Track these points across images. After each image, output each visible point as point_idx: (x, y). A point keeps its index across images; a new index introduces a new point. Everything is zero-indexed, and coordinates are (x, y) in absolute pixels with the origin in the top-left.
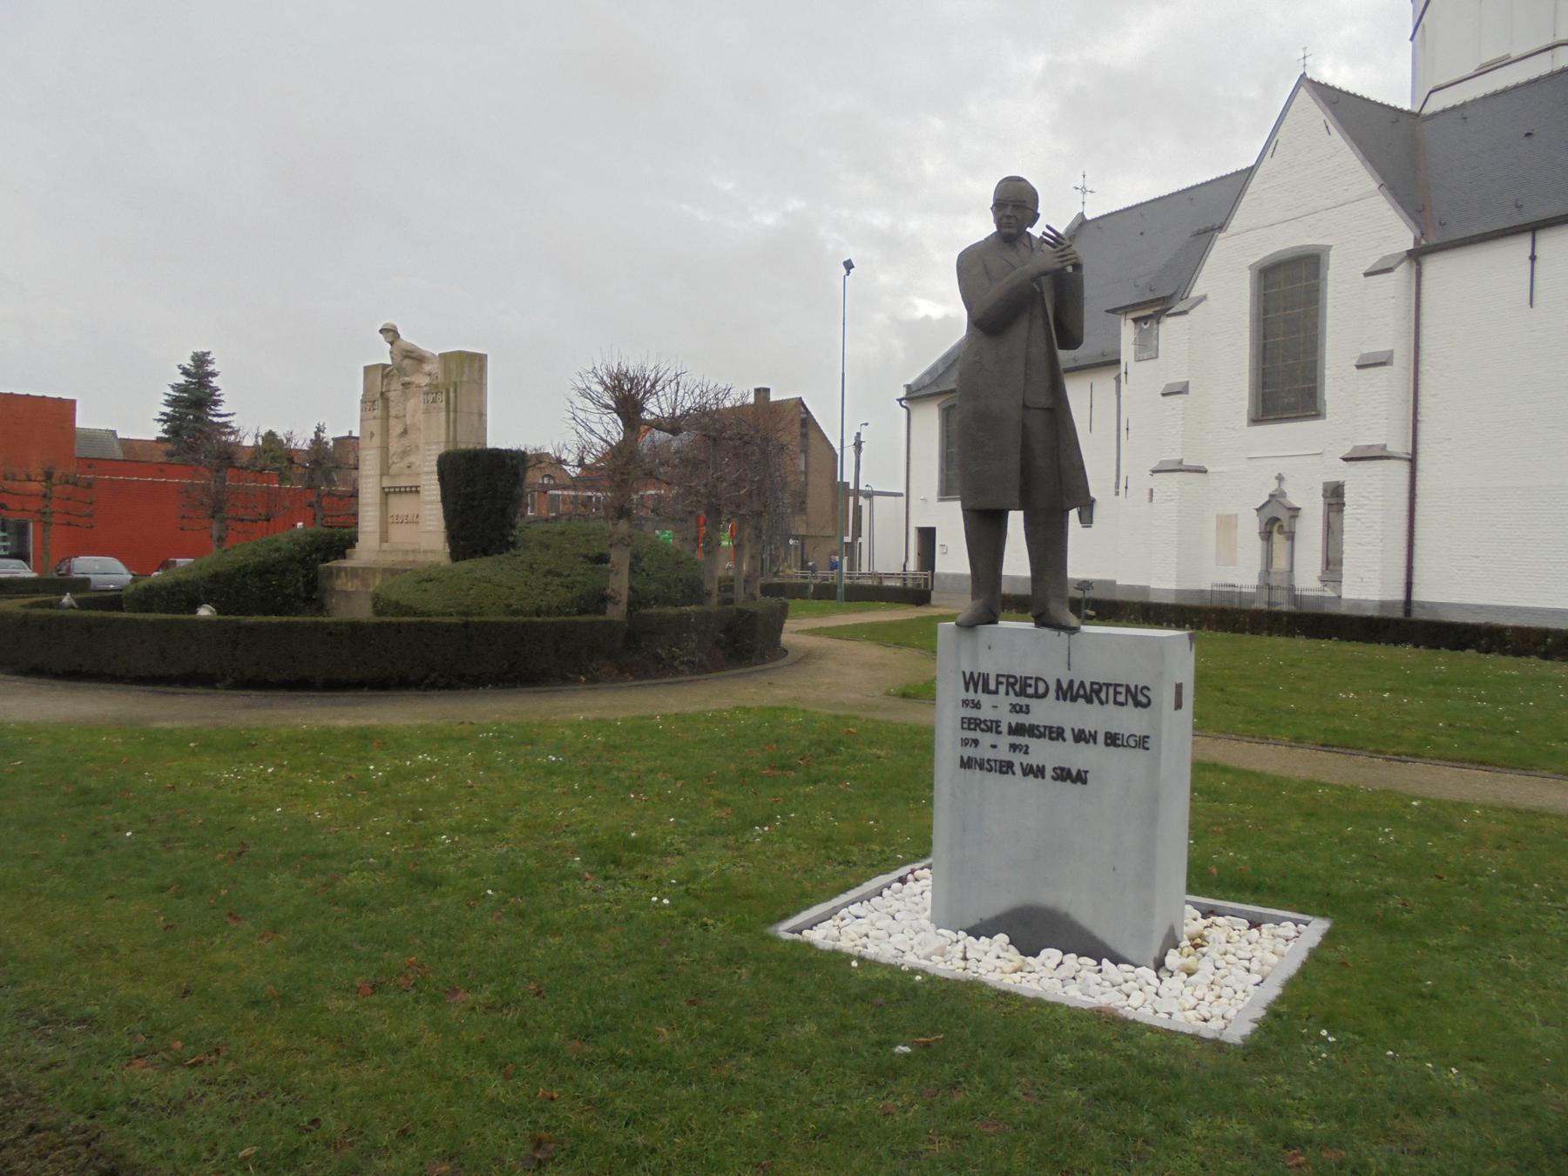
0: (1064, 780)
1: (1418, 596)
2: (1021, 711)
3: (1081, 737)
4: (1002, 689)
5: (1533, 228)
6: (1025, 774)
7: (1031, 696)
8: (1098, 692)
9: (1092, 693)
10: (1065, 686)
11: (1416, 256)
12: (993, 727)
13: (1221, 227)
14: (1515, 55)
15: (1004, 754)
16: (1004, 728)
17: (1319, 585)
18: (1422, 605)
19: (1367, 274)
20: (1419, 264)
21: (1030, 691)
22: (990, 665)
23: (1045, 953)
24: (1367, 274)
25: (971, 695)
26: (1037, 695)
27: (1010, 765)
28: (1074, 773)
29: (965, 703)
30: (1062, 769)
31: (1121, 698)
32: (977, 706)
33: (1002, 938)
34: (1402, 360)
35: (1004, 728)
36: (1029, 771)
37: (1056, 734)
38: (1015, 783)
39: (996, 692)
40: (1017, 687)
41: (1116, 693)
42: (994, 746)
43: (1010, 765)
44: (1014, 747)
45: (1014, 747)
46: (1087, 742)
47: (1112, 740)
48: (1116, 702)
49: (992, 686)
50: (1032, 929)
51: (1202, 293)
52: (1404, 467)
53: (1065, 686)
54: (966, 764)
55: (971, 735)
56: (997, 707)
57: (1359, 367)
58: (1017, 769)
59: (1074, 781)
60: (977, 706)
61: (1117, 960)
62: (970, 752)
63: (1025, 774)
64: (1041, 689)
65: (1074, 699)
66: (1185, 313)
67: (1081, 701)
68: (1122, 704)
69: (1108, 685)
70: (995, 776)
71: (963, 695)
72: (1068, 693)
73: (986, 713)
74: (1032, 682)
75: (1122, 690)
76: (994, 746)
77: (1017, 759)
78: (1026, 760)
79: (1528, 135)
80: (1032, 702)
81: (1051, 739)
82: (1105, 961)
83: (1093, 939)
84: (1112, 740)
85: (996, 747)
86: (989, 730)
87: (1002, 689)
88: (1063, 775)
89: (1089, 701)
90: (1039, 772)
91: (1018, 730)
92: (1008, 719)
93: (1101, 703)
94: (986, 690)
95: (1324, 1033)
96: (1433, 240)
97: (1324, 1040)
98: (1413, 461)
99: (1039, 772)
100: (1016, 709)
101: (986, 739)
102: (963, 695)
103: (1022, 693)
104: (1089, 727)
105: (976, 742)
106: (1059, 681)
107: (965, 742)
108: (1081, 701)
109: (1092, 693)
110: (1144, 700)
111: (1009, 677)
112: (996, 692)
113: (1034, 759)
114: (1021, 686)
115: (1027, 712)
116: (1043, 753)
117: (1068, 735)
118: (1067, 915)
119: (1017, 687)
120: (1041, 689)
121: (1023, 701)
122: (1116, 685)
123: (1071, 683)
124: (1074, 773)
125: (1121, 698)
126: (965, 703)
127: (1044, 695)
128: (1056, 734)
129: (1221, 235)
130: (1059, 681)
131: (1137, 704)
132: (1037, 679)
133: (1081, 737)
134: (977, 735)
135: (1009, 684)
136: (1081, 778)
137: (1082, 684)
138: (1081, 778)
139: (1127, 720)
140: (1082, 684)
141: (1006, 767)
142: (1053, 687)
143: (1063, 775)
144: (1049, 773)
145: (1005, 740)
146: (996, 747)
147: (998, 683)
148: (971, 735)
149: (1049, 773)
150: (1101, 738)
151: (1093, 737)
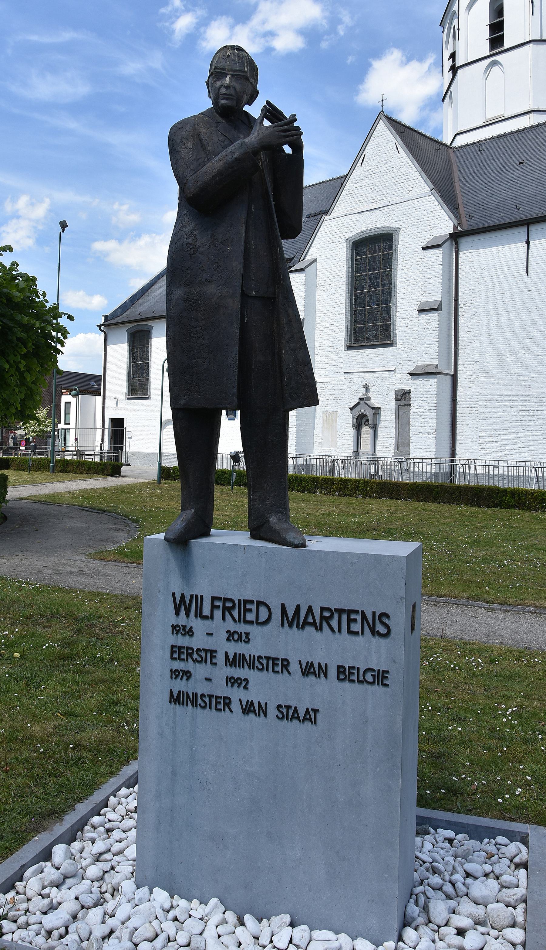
3: (308, 670)
4: (218, 614)
5: (527, 223)
7: (251, 622)
8: (328, 620)
11: (455, 238)
12: (208, 656)
13: (326, 212)
19: (424, 248)
20: (457, 244)
21: (251, 617)
24: (424, 248)
25: (182, 620)
27: (227, 702)
29: (176, 629)
34: (448, 308)
35: (220, 658)
36: (248, 708)
38: (235, 718)
40: (235, 613)
41: (350, 621)
44: (232, 681)
45: (232, 681)
47: (345, 674)
48: (350, 632)
49: (207, 611)
51: (314, 257)
52: (448, 381)
54: (177, 698)
58: (236, 706)
60: (190, 632)
62: (180, 685)
64: (264, 614)
66: (302, 270)
68: (356, 633)
69: (340, 612)
70: (209, 714)
71: (172, 619)
73: (198, 641)
74: (253, 607)
75: (358, 617)
76: (208, 680)
77: (237, 695)
79: (520, 163)
87: (218, 614)
88: (288, 713)
91: (233, 661)
96: (466, 228)
98: (454, 377)
100: (231, 636)
101: (200, 671)
102: (172, 619)
105: (188, 675)
107: (175, 674)
109: (324, 619)
110: (383, 631)
111: (225, 600)
112: (212, 617)
113: (254, 695)
116: (263, 687)
117: (294, 667)
120: (264, 614)
121: (242, 628)
122: (350, 612)
126: (176, 629)
127: (267, 622)
129: (327, 217)
132: (259, 603)
133: (308, 670)
134: (190, 666)
135: (225, 609)
136: (310, 716)
137: (310, 610)
138: (310, 716)
139: (366, 651)
143: (288, 713)
147: (214, 607)
150: (333, 672)
151: (323, 671)
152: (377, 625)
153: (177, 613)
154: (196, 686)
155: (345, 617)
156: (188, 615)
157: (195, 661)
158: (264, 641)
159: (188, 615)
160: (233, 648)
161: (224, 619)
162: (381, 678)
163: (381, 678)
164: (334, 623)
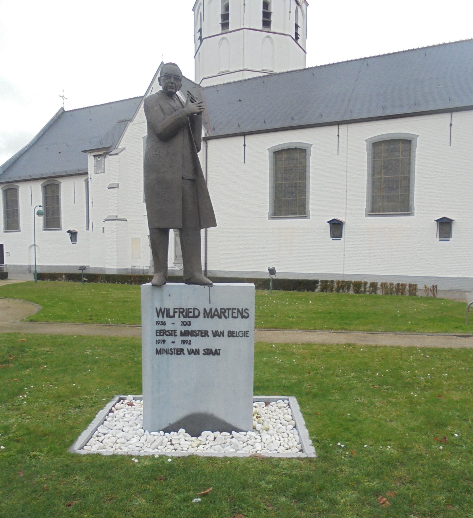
0: (209, 354)
1: (208, 269)
2: (186, 324)
3: (216, 334)
4: (177, 315)
5: (244, 134)
6: (189, 353)
8: (224, 313)
9: (221, 314)
10: (208, 311)
12: (173, 333)
13: (130, 120)
15: (178, 345)
16: (178, 333)
17: (173, 265)
18: (210, 272)
20: (206, 143)
21: (191, 315)
22: (170, 304)
23: (205, 433)
25: (160, 319)
26: (194, 317)
27: (182, 350)
28: (214, 351)
29: (158, 323)
30: (208, 350)
31: (235, 315)
32: (164, 324)
33: (182, 431)
35: (178, 333)
36: (191, 352)
37: (204, 334)
38: (185, 358)
39: (174, 316)
40: (184, 314)
41: (233, 313)
42: (173, 342)
43: (182, 350)
44: (183, 342)
45: (183, 342)
46: (219, 336)
47: (231, 334)
48: (233, 317)
49: (172, 314)
50: (195, 424)
51: (123, 147)
53: (208, 311)
54: (159, 352)
55: (161, 338)
56: (174, 324)
58: (186, 352)
59: (214, 355)
60: (164, 324)
61: (238, 431)
62: (161, 346)
63: (189, 353)
64: (196, 313)
65: (212, 317)
66: (117, 154)
67: (216, 318)
68: (235, 318)
69: (229, 309)
71: (156, 319)
72: (209, 314)
73: (168, 327)
74: (192, 311)
75: (236, 311)
76: (173, 342)
78: (189, 347)
79: (240, 100)
80: (192, 320)
81: (202, 336)
82: (233, 432)
83: (225, 423)
84: (231, 334)
85: (171, 343)
86: (171, 335)
87: (177, 315)
88: (208, 352)
89: (220, 317)
90: (196, 352)
91: (183, 334)
92: (180, 328)
93: (226, 318)
94: (168, 316)
95: (339, 444)
96: (211, 135)
97: (340, 447)
99: (196, 352)
100: (184, 324)
101: (169, 339)
102: (156, 319)
103: (187, 316)
104: (220, 329)
105: (164, 341)
106: (205, 309)
107: (158, 342)
108: (216, 318)
109: (221, 314)
110: (246, 315)
111: (180, 309)
113: (193, 346)
114: (187, 313)
115: (190, 325)
116: (198, 343)
117: (210, 334)
118: (212, 415)
119: (184, 314)
120: (196, 313)
121: (187, 320)
122: (233, 309)
123: (211, 309)
124: (214, 351)
125: (235, 315)
126: (158, 323)
127: (198, 316)
128: (204, 334)
129: (131, 123)
130: (205, 309)
131: (243, 317)
132: (194, 309)
133: (216, 334)
134: (165, 338)
135: (180, 312)
136: (217, 353)
137: (216, 310)
138: (217, 353)
139: (238, 324)
140: (216, 310)
141: (180, 352)
142: (202, 312)
143: (208, 352)
144: (201, 352)
145: (179, 339)
146: (171, 343)
147: (175, 312)
148: (161, 338)
149: (201, 352)
150: (226, 334)
151: (222, 334)
152: (243, 314)
153: (158, 316)
154: (168, 345)
155: (230, 311)
156: (163, 317)
157: (167, 335)
158: (198, 324)
159: (163, 317)
160: (184, 328)
161: (179, 317)
162: (246, 334)
163: (246, 334)
164: (226, 314)
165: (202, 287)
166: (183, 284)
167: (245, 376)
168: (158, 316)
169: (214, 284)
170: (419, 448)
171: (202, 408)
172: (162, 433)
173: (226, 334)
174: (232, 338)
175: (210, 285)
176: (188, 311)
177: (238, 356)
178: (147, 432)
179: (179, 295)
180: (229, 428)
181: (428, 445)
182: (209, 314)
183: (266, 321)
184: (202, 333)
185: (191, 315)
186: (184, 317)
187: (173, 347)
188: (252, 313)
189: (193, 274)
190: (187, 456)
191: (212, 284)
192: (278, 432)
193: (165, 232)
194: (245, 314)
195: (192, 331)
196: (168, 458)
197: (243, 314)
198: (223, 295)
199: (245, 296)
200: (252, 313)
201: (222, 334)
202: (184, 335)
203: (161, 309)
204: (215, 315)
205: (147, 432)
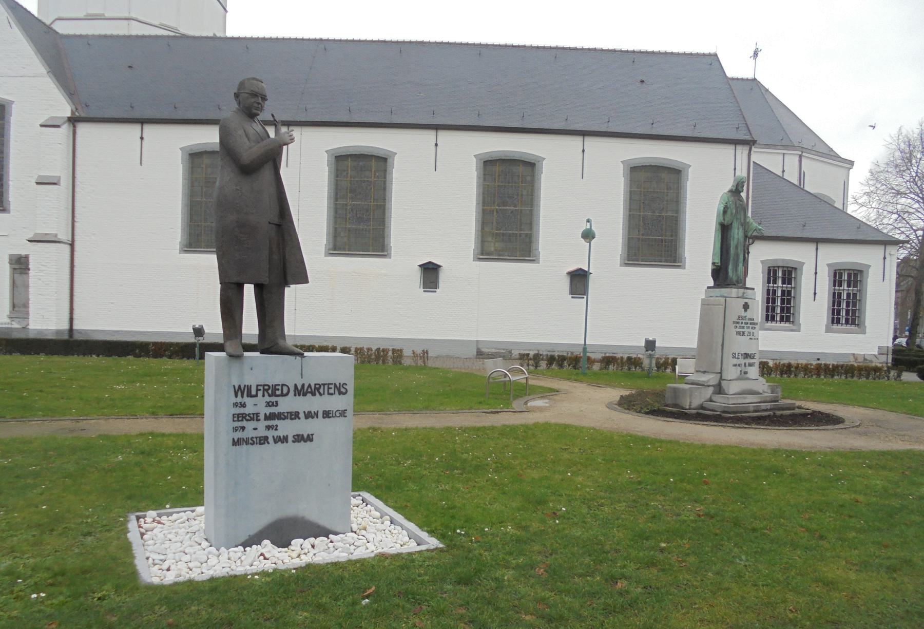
0: (299, 441)
1: (75, 327)
2: (273, 405)
3: (309, 415)
4: (260, 393)
6: (276, 442)
7: (278, 396)
8: (318, 389)
9: (315, 390)
10: (299, 388)
11: (74, 121)
12: (255, 417)
14: (107, 15)
15: (262, 432)
16: (262, 417)
17: (8, 320)
18: (80, 331)
19: (42, 126)
20: (74, 126)
21: (278, 393)
22: (251, 380)
23: (293, 542)
24: (42, 126)
25: (239, 399)
26: (282, 395)
27: (266, 438)
28: (305, 436)
29: (235, 405)
30: (298, 435)
31: (331, 391)
32: (243, 405)
33: (266, 542)
34: (65, 182)
35: (262, 417)
37: (295, 416)
38: (271, 447)
39: (256, 396)
40: (270, 392)
41: (329, 388)
42: (255, 429)
43: (266, 438)
45: (268, 428)
46: (313, 418)
47: (327, 414)
48: (329, 394)
49: (254, 393)
50: (282, 532)
52: (67, 248)
53: (299, 388)
54: (236, 443)
55: (240, 424)
56: (257, 405)
57: (37, 183)
58: (271, 440)
59: (305, 441)
60: (243, 405)
61: (336, 534)
62: (239, 435)
63: (276, 442)
64: (285, 391)
65: (304, 395)
67: (309, 395)
68: (332, 394)
69: (324, 385)
70: (257, 447)
71: (234, 400)
72: (301, 391)
73: (250, 409)
74: (280, 387)
75: (332, 386)
76: (255, 429)
77: (271, 434)
78: (276, 434)
80: (280, 400)
81: (291, 419)
82: (331, 536)
83: (319, 527)
84: (327, 414)
85: (251, 429)
86: (252, 419)
87: (260, 393)
88: (299, 438)
89: (314, 394)
90: (284, 439)
91: (268, 417)
92: (264, 410)
93: (320, 394)
94: (250, 395)
95: (458, 531)
97: (460, 534)
98: (72, 245)
99: (284, 439)
100: (269, 404)
101: (249, 425)
102: (234, 400)
103: (274, 394)
104: (313, 409)
105: (243, 428)
106: (296, 385)
107: (235, 429)
108: (309, 395)
109: (315, 390)
110: (344, 390)
111: (264, 385)
112: (256, 396)
113: (280, 433)
114: (273, 391)
115: (277, 405)
116: (287, 428)
117: (302, 415)
118: (303, 518)
119: (270, 392)
120: (285, 391)
121: (274, 399)
122: (329, 384)
123: (303, 385)
124: (305, 436)
125: (331, 391)
126: (235, 405)
128: (295, 416)
130: (296, 385)
131: (340, 393)
132: (283, 385)
133: (309, 415)
134: (244, 423)
136: (310, 438)
137: (310, 386)
138: (310, 438)
139: (335, 402)
140: (310, 386)
141: (263, 440)
142: (292, 389)
143: (299, 438)
144: (290, 439)
145: (263, 424)
146: (251, 429)
147: (258, 390)
148: (240, 424)
149: (290, 439)
150: (320, 414)
151: (316, 414)
152: (340, 389)
153: (236, 396)
154: (249, 433)
155: (326, 387)
156: (242, 397)
157: (247, 420)
158: (286, 404)
159: (242, 397)
160: (269, 410)
161: (264, 396)
162: (343, 413)
163: (343, 413)
164: (321, 391)
165: (293, 358)
166: (258, 354)
167: (341, 467)
168: (236, 396)
169: (306, 354)
170: (535, 526)
171: (290, 511)
172: (241, 548)
173: (320, 414)
174: (327, 419)
175: (302, 355)
176: (275, 388)
177: (334, 441)
178: (223, 549)
179: (262, 369)
180: (325, 532)
181: (543, 521)
182: (301, 391)
183: (367, 398)
184: (291, 415)
185: (278, 393)
186: (269, 396)
187: (254, 436)
188: (351, 388)
189: (271, 341)
190: (304, 565)
191: (303, 354)
192: (376, 532)
193: (240, 287)
194: (343, 390)
195: (280, 414)
196: (291, 570)
197: (340, 389)
198: (319, 369)
199: (340, 368)
200: (351, 388)
201: (316, 414)
202: (264, 420)
203: (240, 386)
204: (308, 392)
205: (223, 549)
